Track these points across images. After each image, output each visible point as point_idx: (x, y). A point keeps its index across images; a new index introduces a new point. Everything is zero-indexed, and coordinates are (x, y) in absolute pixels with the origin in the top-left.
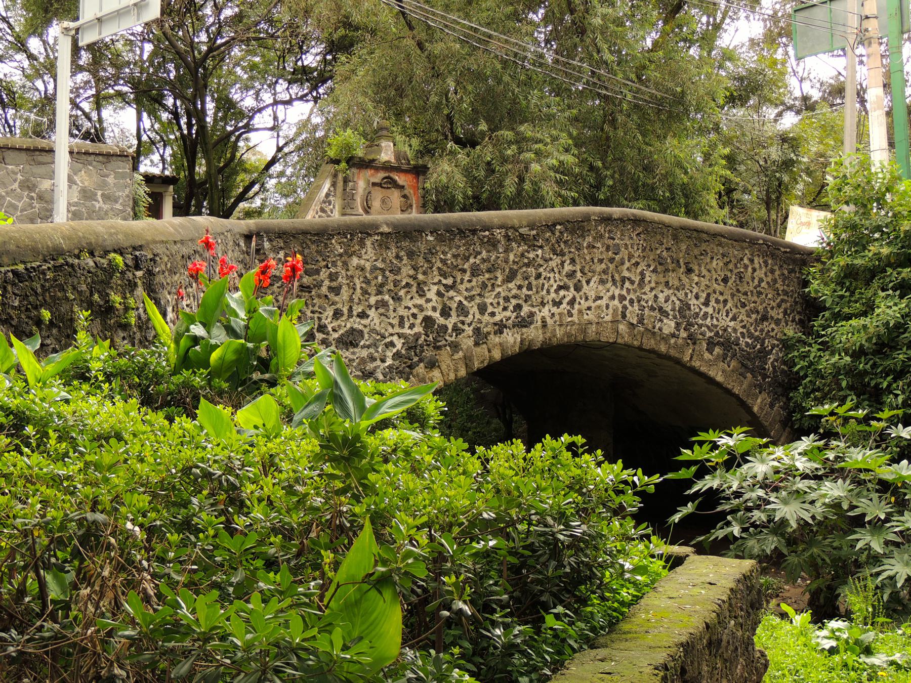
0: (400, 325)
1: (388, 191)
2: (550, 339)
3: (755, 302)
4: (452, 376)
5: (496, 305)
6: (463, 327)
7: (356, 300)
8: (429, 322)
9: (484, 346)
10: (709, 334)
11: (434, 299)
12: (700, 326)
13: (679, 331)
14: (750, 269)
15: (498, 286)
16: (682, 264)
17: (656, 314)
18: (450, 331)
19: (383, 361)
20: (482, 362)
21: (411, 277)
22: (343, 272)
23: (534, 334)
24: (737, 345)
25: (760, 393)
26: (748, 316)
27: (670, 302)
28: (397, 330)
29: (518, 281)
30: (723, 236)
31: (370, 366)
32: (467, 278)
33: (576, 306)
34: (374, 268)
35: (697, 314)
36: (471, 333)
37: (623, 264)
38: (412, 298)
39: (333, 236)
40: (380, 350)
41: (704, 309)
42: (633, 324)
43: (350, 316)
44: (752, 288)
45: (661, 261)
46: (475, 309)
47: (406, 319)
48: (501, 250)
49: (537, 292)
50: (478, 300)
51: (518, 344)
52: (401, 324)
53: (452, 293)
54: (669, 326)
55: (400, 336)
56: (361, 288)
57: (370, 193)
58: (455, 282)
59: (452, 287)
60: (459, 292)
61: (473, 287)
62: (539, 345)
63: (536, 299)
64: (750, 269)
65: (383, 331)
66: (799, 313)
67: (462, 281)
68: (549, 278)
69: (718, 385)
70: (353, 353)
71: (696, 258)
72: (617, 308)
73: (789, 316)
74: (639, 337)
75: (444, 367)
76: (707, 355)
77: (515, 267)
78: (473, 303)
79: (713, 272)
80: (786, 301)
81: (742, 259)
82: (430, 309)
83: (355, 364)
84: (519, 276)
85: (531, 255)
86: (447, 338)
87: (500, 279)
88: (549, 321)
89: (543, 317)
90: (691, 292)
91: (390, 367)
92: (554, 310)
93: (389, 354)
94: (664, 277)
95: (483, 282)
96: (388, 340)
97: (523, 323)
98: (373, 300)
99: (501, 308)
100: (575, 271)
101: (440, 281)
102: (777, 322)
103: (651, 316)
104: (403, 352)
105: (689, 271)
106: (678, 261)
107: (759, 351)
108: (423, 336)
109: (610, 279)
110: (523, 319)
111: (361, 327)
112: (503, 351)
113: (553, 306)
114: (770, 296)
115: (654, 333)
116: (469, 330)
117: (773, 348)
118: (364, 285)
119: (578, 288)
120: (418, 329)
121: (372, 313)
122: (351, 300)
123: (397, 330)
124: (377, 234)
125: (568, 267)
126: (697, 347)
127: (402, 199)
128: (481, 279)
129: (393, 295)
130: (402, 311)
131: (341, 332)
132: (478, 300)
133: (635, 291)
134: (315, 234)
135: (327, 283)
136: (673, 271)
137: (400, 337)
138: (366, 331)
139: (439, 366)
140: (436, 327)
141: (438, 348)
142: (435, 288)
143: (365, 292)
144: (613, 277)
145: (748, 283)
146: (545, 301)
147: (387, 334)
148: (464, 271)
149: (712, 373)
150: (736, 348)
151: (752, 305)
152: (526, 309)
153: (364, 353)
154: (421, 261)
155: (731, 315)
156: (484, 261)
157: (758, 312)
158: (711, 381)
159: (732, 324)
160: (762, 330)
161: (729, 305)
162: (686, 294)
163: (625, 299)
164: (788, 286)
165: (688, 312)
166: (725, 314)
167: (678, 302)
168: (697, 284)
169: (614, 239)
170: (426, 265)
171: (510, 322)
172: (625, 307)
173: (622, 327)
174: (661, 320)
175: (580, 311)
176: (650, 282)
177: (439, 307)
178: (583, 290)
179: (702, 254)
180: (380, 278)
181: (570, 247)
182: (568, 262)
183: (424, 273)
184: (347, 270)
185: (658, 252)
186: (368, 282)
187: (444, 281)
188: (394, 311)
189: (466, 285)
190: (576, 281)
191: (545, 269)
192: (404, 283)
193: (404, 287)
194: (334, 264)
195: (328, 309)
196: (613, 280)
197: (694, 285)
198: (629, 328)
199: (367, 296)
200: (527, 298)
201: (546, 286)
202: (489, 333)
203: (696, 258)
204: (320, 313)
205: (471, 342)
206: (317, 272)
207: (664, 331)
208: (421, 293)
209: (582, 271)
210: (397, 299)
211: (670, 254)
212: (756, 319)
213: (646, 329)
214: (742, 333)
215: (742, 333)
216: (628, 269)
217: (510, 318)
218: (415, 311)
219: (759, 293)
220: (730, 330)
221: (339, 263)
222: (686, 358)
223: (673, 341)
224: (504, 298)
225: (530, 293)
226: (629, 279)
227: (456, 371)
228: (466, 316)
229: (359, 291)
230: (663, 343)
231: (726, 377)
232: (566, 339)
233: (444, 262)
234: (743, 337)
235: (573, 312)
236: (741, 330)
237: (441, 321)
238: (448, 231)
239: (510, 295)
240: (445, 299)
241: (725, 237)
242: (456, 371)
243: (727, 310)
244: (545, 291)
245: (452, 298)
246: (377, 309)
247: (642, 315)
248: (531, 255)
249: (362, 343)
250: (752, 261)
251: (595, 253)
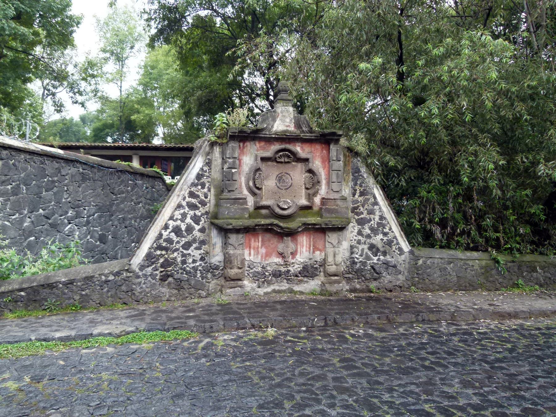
1: (287, 165)
57: (258, 170)
127: (307, 174)
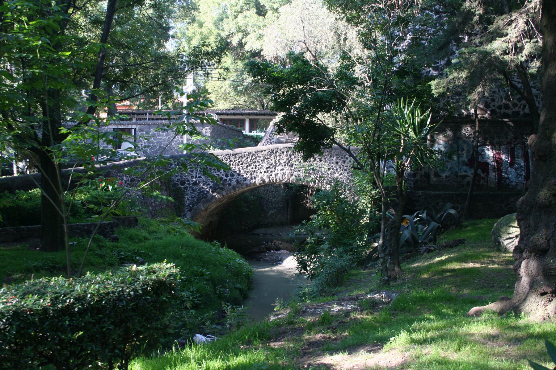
8: (221, 178)
116: (235, 180)
177: (224, 175)
205: (235, 183)
237: (225, 178)
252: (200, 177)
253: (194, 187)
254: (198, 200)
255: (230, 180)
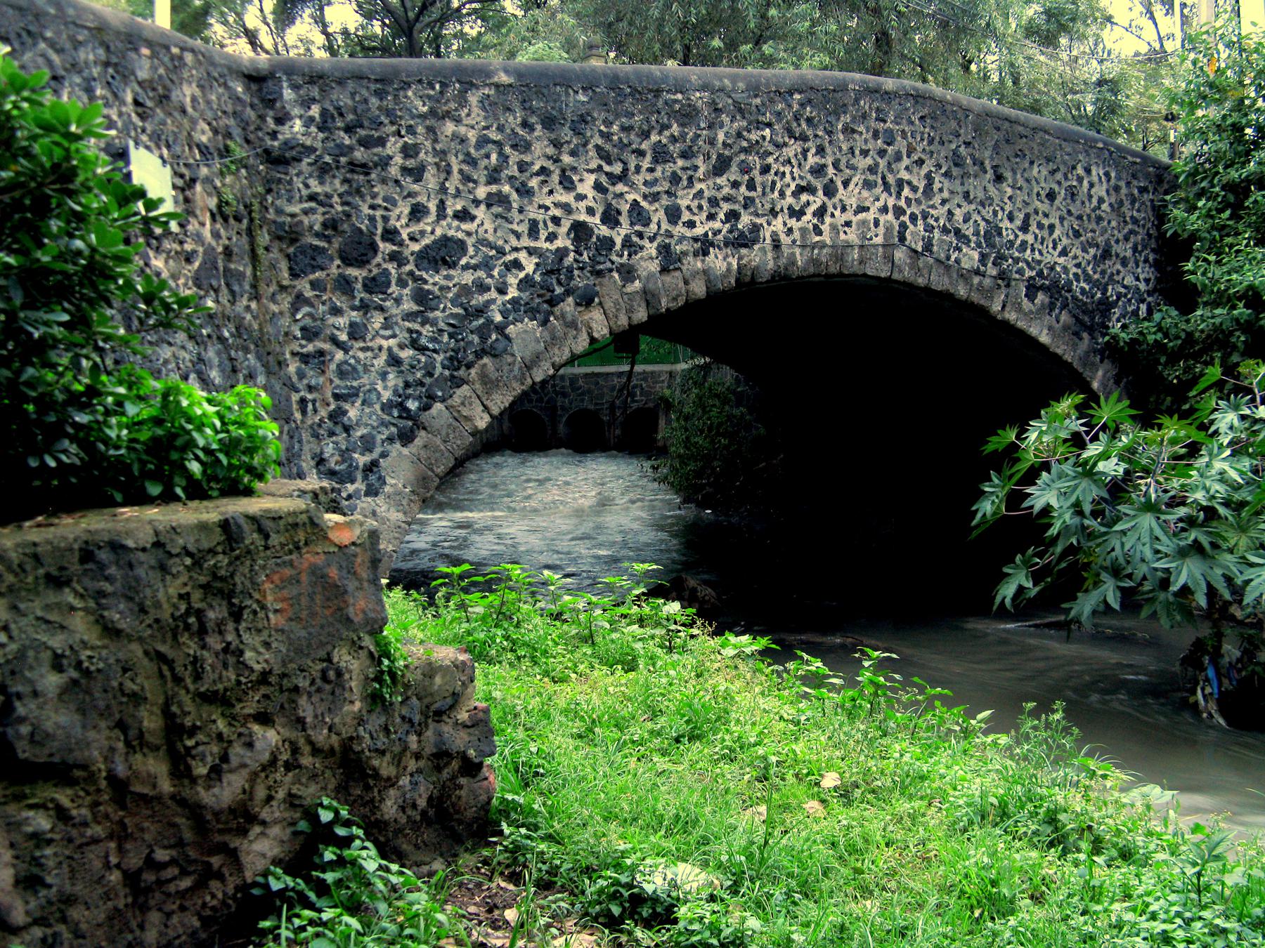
0: (530, 235)
2: (786, 269)
3: (1093, 231)
4: (623, 321)
5: (696, 211)
6: (641, 243)
7: (452, 191)
8: (580, 231)
9: (677, 274)
10: (1028, 273)
11: (590, 196)
12: (1017, 261)
13: (985, 265)
14: (1085, 183)
15: (700, 180)
16: (988, 168)
17: (951, 238)
18: (618, 247)
19: (502, 291)
20: (675, 299)
21: (549, 158)
22: (428, 144)
23: (760, 258)
24: (1069, 291)
25: (1102, 361)
26: (1084, 250)
27: (971, 222)
28: (526, 242)
29: (733, 174)
30: (1046, 132)
31: (479, 300)
32: (646, 164)
33: (828, 220)
34: (483, 141)
35: (1011, 243)
36: (654, 253)
37: (898, 158)
38: (551, 192)
39: (408, 85)
40: (495, 273)
41: (1021, 236)
42: (915, 252)
43: (441, 215)
44: (1088, 211)
45: (957, 161)
46: (661, 214)
47: (541, 225)
48: (703, 125)
49: (764, 194)
50: (665, 201)
51: (734, 273)
52: (533, 231)
53: (620, 188)
54: (970, 257)
55: (531, 252)
56: (461, 171)
58: (625, 170)
59: (623, 177)
60: (632, 185)
61: (656, 180)
62: (765, 277)
63: (762, 205)
64: (1085, 183)
65: (500, 243)
66: (1153, 250)
67: (638, 169)
68: (784, 173)
69: (1043, 348)
70: (448, 278)
71: (1008, 158)
72: (892, 225)
73: (1140, 253)
74: (925, 272)
75: (609, 304)
76: (1026, 305)
77: (727, 153)
78: (657, 205)
79: (1033, 182)
80: (1136, 233)
81: (1074, 168)
82: (583, 210)
83: (450, 295)
84: (734, 168)
85: (754, 136)
86: (614, 258)
87: (702, 170)
88: (785, 240)
89: (774, 234)
90: (1002, 209)
91: (514, 301)
92: (792, 222)
93: (513, 280)
94: (962, 184)
95: (674, 174)
96: (509, 258)
97: (742, 241)
98: (481, 192)
99: (704, 215)
100: (824, 166)
101: (600, 168)
102: (1124, 262)
103: (943, 241)
104: (538, 278)
105: (999, 178)
106: (982, 163)
107: (1100, 302)
108: (572, 254)
109: (880, 181)
110: (742, 234)
111: (460, 235)
112: (708, 282)
113: (790, 217)
114: (1114, 224)
115: (948, 268)
116: (651, 249)
117: (1118, 298)
118: (465, 167)
119: (830, 191)
120: (562, 242)
121: (480, 212)
122: (443, 189)
123: (526, 242)
124: (489, 85)
125: (812, 160)
126: (1011, 291)
128: (669, 167)
129: (517, 184)
130: (533, 213)
131: (427, 241)
132: (665, 201)
133: (918, 202)
134: (376, 81)
135: (398, 160)
136: (976, 176)
137: (530, 254)
138: (470, 241)
139: (600, 304)
140: (594, 239)
141: (599, 274)
142: (591, 179)
143: (467, 179)
144: (884, 178)
145: (1083, 203)
146: (778, 208)
147: (508, 248)
148: (641, 153)
149: (1033, 331)
150: (1068, 295)
151: (1089, 235)
152: (745, 220)
153: (468, 278)
154: (566, 134)
155: (1059, 248)
156: (674, 139)
157: (1097, 246)
158: (1033, 342)
159: (1062, 260)
160: (1103, 272)
161: (1057, 233)
162: (995, 213)
163: (904, 213)
164: (1138, 211)
165: (997, 239)
166: (1051, 245)
167: (983, 224)
168: (1010, 198)
169: (885, 121)
170: (575, 141)
171: (720, 237)
172: (903, 226)
173: (900, 255)
174: (960, 250)
175: (834, 228)
176: (941, 190)
177: (600, 210)
178: (839, 196)
179: (1017, 156)
180: (494, 157)
181: (815, 127)
182: (813, 150)
183: (573, 153)
184: (436, 141)
185: (953, 146)
186: (472, 162)
187: (607, 168)
188: (521, 211)
189: (644, 176)
190: (826, 180)
191: (776, 160)
192: (536, 167)
193: (537, 174)
194: (411, 130)
195: (400, 203)
196: (885, 183)
197: (1006, 200)
198: (911, 258)
199: (471, 185)
200: (748, 203)
201: (778, 185)
202: (685, 254)
203: (1008, 158)
204: (386, 209)
205: (654, 267)
206: (382, 142)
207: (963, 265)
208: (567, 184)
209: (836, 165)
210: (524, 191)
211: (970, 150)
212: (1095, 257)
213: (938, 261)
214: (1075, 275)
215: (1075, 275)
216: (907, 168)
217: (720, 231)
218: (557, 212)
219: (1099, 219)
220: (1058, 269)
221: (420, 129)
222: (996, 307)
223: (976, 280)
224: (710, 200)
225: (753, 194)
226: (909, 183)
227: (630, 311)
228: (647, 225)
229: (456, 175)
230: (961, 282)
231: (1054, 337)
232: (812, 270)
233: (607, 136)
234: (1078, 280)
235: (822, 227)
236: (1075, 270)
237: (604, 231)
238: (612, 89)
239: (719, 196)
240: (610, 196)
241: (1049, 134)
242: (630, 311)
243: (1054, 241)
244: (776, 194)
245: (621, 195)
246: (489, 206)
247: (930, 239)
248: (754, 136)
249: (463, 261)
250: (1088, 171)
251: (855, 140)
252: (464, 216)
253: (434, 280)
254: (455, 362)
255: (627, 243)
